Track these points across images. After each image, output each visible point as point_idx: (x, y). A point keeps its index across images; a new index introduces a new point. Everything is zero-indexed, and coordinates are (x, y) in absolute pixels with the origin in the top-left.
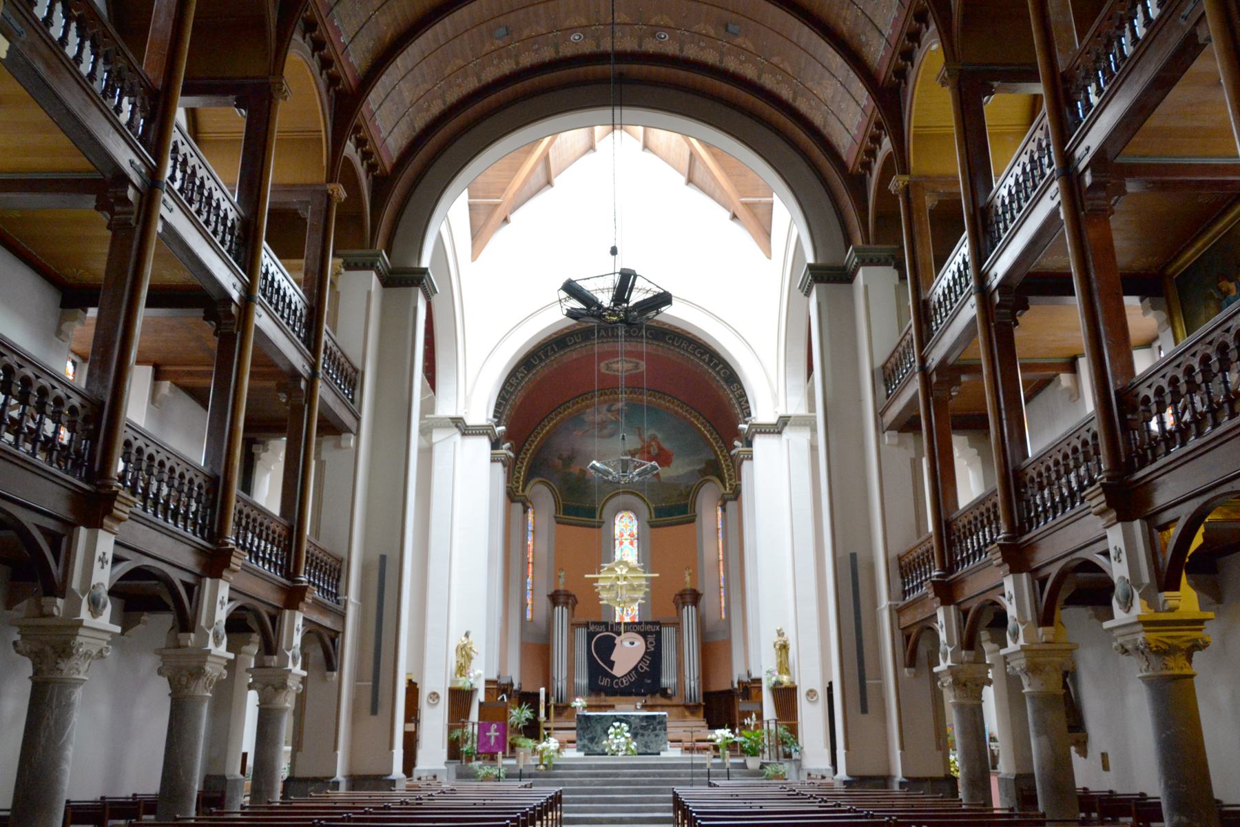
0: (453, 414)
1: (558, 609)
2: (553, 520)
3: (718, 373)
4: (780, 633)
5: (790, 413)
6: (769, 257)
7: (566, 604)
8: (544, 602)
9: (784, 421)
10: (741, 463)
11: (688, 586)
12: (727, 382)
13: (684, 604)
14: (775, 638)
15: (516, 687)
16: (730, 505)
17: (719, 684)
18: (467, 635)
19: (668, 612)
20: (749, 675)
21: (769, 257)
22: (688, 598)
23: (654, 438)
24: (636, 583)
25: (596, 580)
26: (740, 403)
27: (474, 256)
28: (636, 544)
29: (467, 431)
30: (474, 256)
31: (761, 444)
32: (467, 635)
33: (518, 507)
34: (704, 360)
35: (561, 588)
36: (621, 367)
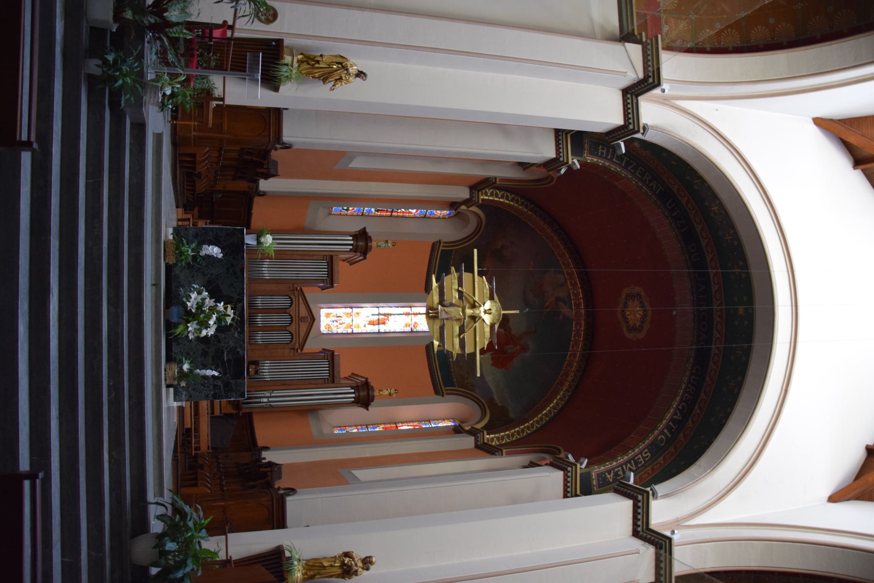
0: (665, 73)
1: (349, 240)
2: (435, 240)
3: (662, 433)
4: (367, 562)
5: (677, 552)
6: (834, 498)
7: (355, 250)
8: (356, 228)
9: (661, 544)
10: (557, 465)
11: (376, 393)
12: (652, 444)
13: (356, 388)
14: (360, 553)
15: (265, 185)
16: (468, 442)
17: (263, 432)
18: (360, 74)
19: (344, 370)
20: (292, 491)
21: (834, 498)
22: (363, 394)
23: (525, 348)
24: (468, 336)
25: (470, 269)
26: (629, 461)
27: (820, 122)
28: (408, 329)
29: (631, 94)
30: (820, 122)
31: (616, 510)
32: (360, 74)
33: (464, 193)
34: (675, 414)
35: (374, 244)
36: (634, 312)
